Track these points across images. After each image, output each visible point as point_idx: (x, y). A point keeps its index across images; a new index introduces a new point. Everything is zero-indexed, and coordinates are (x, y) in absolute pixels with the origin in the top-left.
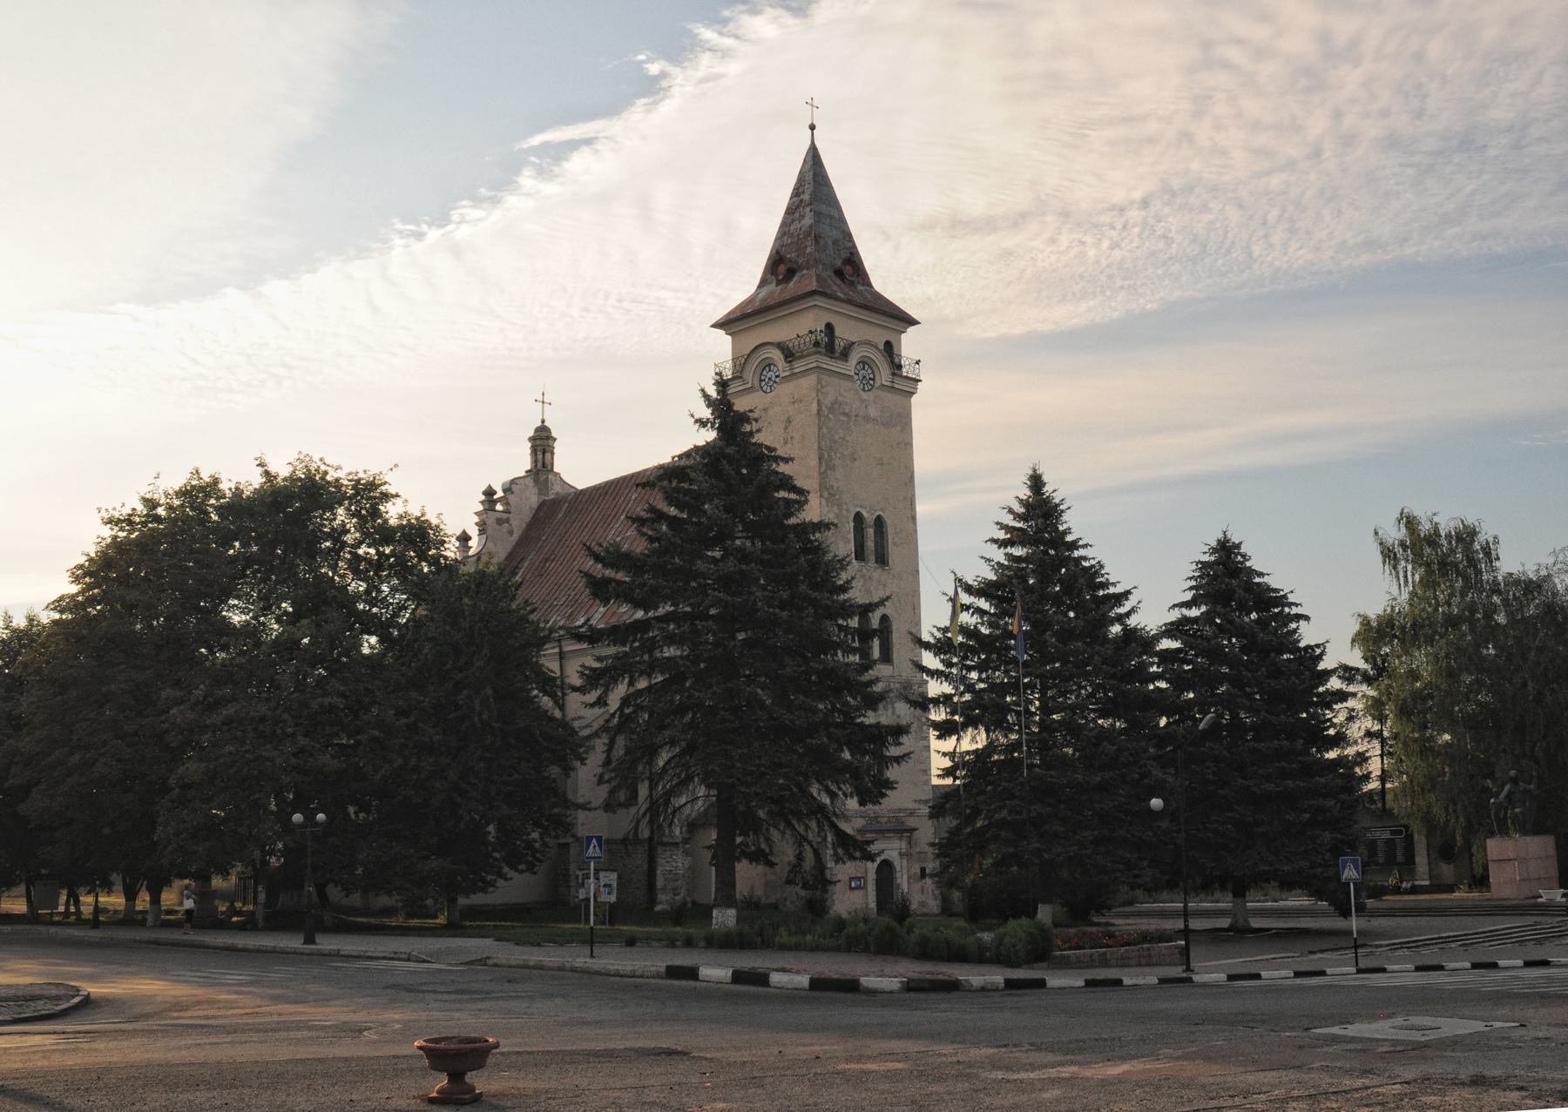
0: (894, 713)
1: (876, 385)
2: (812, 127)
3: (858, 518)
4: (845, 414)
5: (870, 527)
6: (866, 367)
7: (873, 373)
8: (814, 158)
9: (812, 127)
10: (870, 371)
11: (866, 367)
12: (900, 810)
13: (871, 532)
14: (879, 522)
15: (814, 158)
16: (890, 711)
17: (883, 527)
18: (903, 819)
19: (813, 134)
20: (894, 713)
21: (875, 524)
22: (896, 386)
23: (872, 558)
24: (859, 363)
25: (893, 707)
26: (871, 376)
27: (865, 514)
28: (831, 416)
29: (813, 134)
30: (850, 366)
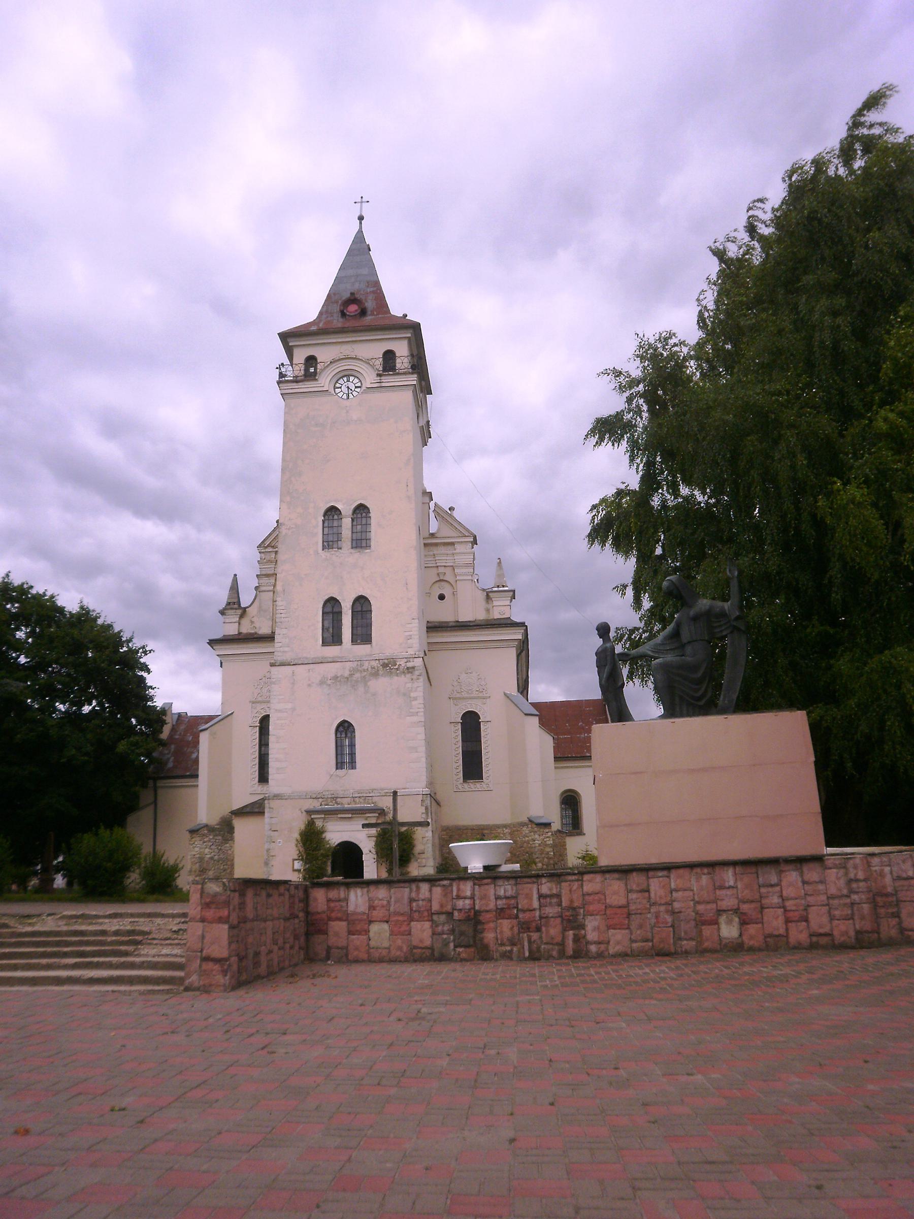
2: (361, 218)
3: (332, 512)
5: (346, 517)
6: (352, 378)
8: (359, 238)
9: (361, 218)
10: (356, 380)
11: (352, 378)
13: (347, 522)
14: (361, 510)
15: (359, 238)
16: (361, 689)
18: (375, 799)
19: (361, 223)
22: (383, 384)
25: (366, 685)
26: (359, 384)
29: (361, 223)
30: (325, 381)
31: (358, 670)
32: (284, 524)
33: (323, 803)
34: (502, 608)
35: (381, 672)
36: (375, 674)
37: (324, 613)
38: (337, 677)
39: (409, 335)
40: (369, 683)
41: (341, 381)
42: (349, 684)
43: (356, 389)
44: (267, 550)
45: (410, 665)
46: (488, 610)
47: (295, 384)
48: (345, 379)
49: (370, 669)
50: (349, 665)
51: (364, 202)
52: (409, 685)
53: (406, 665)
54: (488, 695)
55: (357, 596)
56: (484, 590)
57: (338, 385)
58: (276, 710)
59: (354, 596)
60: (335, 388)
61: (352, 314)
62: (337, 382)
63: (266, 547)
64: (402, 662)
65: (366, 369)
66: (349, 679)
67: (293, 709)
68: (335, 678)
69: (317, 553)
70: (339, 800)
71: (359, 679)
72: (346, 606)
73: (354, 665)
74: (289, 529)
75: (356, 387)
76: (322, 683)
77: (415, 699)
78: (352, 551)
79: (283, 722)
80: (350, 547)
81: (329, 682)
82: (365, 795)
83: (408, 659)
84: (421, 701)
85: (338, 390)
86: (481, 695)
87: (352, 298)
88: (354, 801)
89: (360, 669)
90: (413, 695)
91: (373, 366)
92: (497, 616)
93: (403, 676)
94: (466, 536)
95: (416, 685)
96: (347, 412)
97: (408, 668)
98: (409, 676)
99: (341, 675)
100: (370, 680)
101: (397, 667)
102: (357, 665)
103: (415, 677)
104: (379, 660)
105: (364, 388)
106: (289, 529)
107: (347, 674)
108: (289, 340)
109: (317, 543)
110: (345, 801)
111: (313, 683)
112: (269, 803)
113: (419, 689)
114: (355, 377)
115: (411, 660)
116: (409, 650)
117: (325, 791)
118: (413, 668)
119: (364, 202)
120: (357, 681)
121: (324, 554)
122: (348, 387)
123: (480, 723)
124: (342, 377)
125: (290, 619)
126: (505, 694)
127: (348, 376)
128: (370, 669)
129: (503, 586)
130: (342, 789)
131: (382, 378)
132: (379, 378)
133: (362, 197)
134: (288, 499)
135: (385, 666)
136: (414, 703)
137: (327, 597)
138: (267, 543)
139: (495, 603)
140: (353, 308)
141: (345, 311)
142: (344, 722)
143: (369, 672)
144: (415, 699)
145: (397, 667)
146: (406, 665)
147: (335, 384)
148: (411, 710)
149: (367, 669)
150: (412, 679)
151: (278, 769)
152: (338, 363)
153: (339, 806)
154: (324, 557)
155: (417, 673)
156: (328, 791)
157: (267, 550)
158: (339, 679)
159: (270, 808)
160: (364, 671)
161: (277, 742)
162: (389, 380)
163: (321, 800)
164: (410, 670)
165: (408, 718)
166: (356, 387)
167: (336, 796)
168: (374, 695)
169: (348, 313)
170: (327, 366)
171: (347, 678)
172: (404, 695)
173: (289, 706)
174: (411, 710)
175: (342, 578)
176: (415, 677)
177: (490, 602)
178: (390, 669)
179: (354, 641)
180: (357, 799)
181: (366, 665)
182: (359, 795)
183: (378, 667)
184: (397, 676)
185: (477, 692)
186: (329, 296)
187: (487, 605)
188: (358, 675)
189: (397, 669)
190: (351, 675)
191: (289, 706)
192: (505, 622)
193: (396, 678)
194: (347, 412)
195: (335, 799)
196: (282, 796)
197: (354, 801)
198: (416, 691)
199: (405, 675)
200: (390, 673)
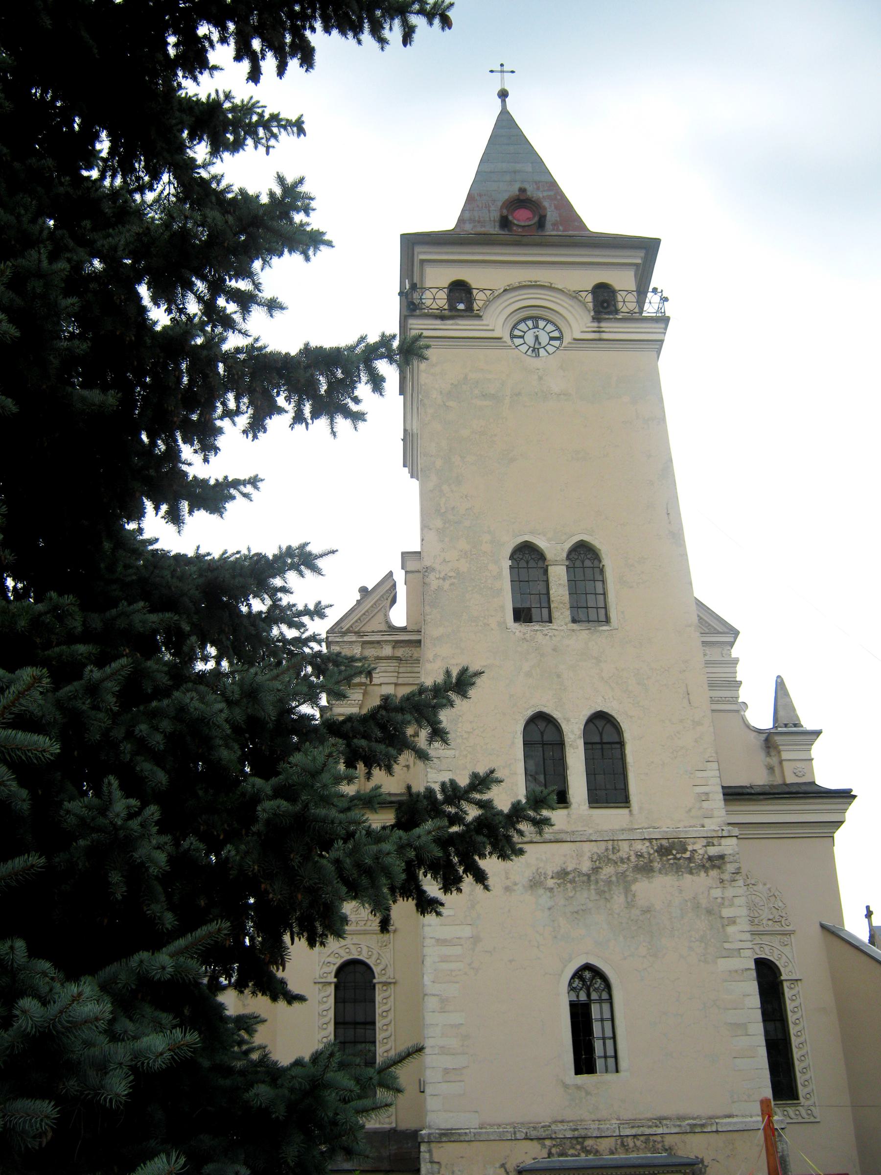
0: (630, 905)
1: (565, 344)
2: (503, 95)
4: (484, 396)
5: (556, 563)
6: (542, 324)
7: (558, 329)
9: (503, 95)
10: (550, 328)
11: (542, 324)
12: (660, 1120)
13: (558, 575)
16: (618, 899)
17: (600, 561)
18: (669, 1141)
19: (504, 102)
20: (630, 904)
21: (568, 557)
22: (605, 336)
23: (562, 613)
24: (524, 320)
25: (627, 890)
26: (556, 334)
27: (541, 543)
28: (451, 403)
29: (504, 102)
31: (609, 859)
32: (433, 570)
33: (554, 1150)
34: (799, 764)
35: (656, 865)
36: (646, 869)
37: (526, 744)
38: (567, 873)
39: (639, 261)
40: (634, 888)
41: (522, 326)
42: (592, 887)
43: (551, 342)
44: (346, 639)
45: (713, 851)
46: (771, 769)
47: (438, 322)
48: (530, 323)
49: (633, 858)
50: (588, 849)
51: (507, 72)
52: (717, 893)
53: (706, 852)
54: (787, 928)
55: (592, 711)
56: (759, 731)
57: (516, 332)
58: (438, 940)
59: (587, 713)
60: (513, 337)
61: (523, 224)
62: (514, 327)
63: (344, 634)
64: (699, 846)
65: (570, 308)
66: (593, 878)
67: (476, 939)
68: (562, 874)
69: (502, 625)
70: (589, 1143)
71: (614, 879)
72: (572, 732)
73: (600, 848)
74: (444, 579)
75: (552, 339)
76: (535, 884)
77: (732, 921)
78: (575, 626)
79: (452, 966)
80: (569, 619)
81: (550, 883)
82: (648, 1131)
83: (710, 841)
84: (744, 925)
85: (518, 341)
86: (777, 927)
87: (522, 198)
88: (623, 1144)
89: (614, 857)
90: (726, 912)
91: (584, 304)
92: (790, 779)
93: (703, 874)
94: (721, 633)
95: (730, 892)
96: (540, 378)
97: (710, 858)
98: (714, 873)
99: (575, 869)
100: (635, 880)
101: (688, 855)
102: (607, 850)
103: (726, 876)
104: (650, 840)
105: (567, 339)
106: (444, 579)
107: (586, 866)
108: (417, 249)
109: (502, 608)
110: (604, 1145)
111: (515, 884)
112: (430, 1151)
113: (737, 901)
114: (549, 321)
115: (715, 841)
116: (706, 822)
117: (555, 1122)
118: (722, 857)
119: (507, 72)
120: (609, 883)
121: (520, 629)
122: (537, 337)
123: (781, 982)
124: (524, 320)
125: (457, 753)
126: (823, 927)
127: (535, 319)
128: (633, 858)
129: (795, 725)
130: (593, 1117)
131: (603, 324)
132: (596, 324)
133: (502, 65)
134: (439, 523)
135: (663, 851)
136: (731, 929)
137: (530, 713)
138: (346, 626)
139: (785, 755)
140: (522, 217)
141: (510, 218)
142: (587, 967)
143: (631, 865)
144: (732, 921)
145: (688, 855)
146: (706, 852)
147: (512, 329)
148: (727, 945)
149: (628, 859)
150: (722, 881)
151: (446, 1071)
152: (517, 293)
153: (591, 1157)
154: (517, 633)
155: (730, 868)
156: (562, 1122)
157: (346, 639)
158: (570, 877)
159: (432, 1162)
160: (622, 860)
161: (443, 1011)
162: (613, 329)
163: (548, 1143)
164: (716, 862)
165: (721, 961)
166: (552, 339)
167: (583, 1133)
168: (647, 911)
169: (516, 222)
170: (499, 296)
171: (589, 876)
172: (709, 912)
173: (466, 932)
174: (727, 945)
175: (559, 676)
176: (726, 876)
177: (773, 753)
178: (675, 858)
179: (596, 799)
180: (630, 1142)
181: (624, 846)
182: (633, 1131)
183: (650, 854)
184: (691, 873)
185: (770, 923)
186: (470, 198)
187: (768, 759)
188: (608, 871)
189: (690, 859)
190: (596, 870)
191: (466, 932)
192: (804, 788)
193: (688, 877)
194: (540, 378)
195: (580, 1139)
196: (459, 1134)
197: (623, 1144)
198: (731, 905)
199: (706, 872)
200: (677, 869)
